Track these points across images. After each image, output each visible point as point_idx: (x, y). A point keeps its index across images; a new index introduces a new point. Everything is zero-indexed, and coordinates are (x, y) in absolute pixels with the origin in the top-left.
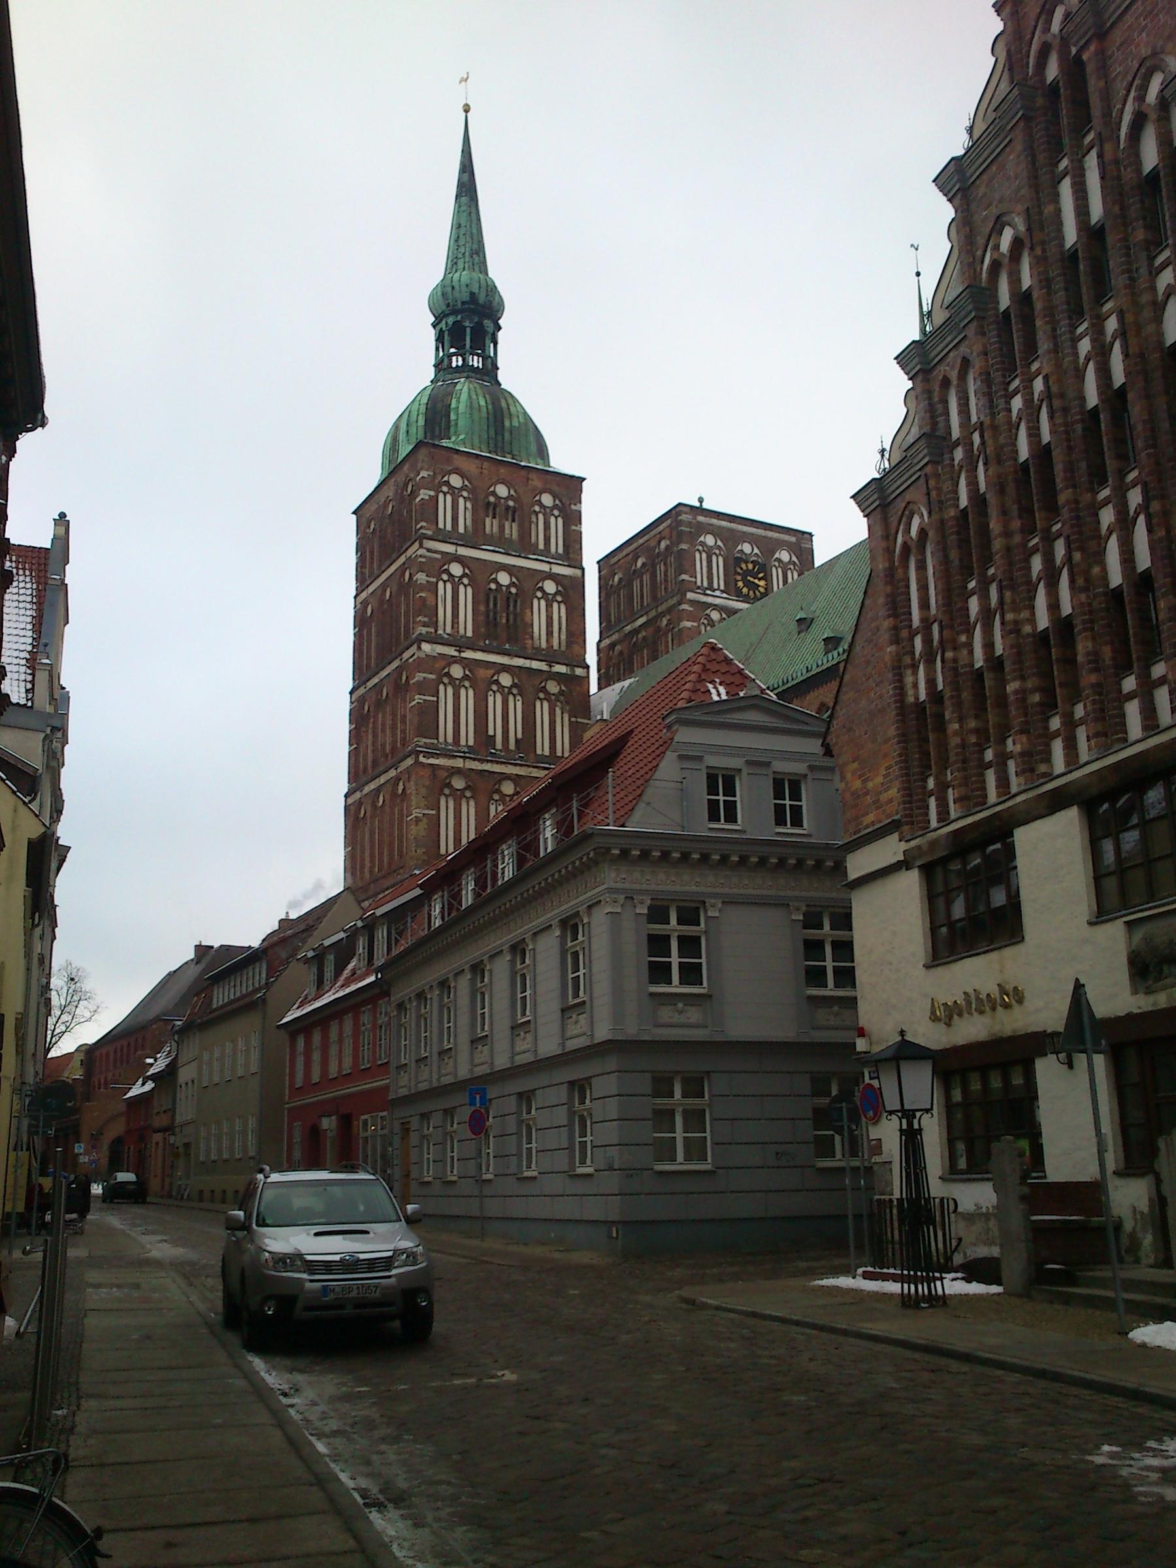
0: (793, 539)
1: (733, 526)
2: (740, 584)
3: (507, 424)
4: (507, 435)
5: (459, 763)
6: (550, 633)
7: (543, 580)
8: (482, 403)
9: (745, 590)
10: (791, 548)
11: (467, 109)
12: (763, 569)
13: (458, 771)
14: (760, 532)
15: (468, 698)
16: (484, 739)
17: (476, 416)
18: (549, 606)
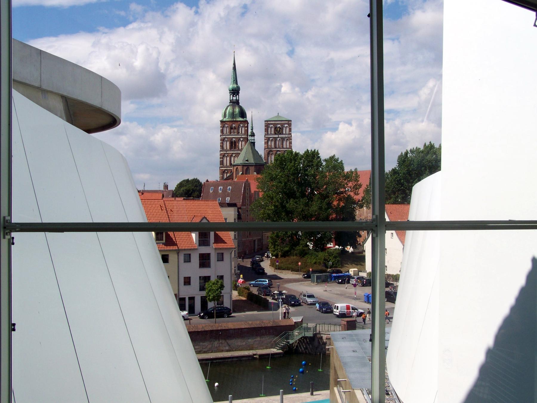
0: (287, 122)
1: (275, 122)
2: (276, 132)
3: (235, 113)
4: (235, 116)
5: (226, 168)
6: (242, 146)
7: (240, 138)
8: (231, 111)
9: (277, 133)
10: (286, 124)
11: (234, 52)
12: (281, 129)
13: (226, 170)
14: (281, 122)
15: (228, 158)
16: (231, 164)
17: (230, 114)
18: (242, 142)
